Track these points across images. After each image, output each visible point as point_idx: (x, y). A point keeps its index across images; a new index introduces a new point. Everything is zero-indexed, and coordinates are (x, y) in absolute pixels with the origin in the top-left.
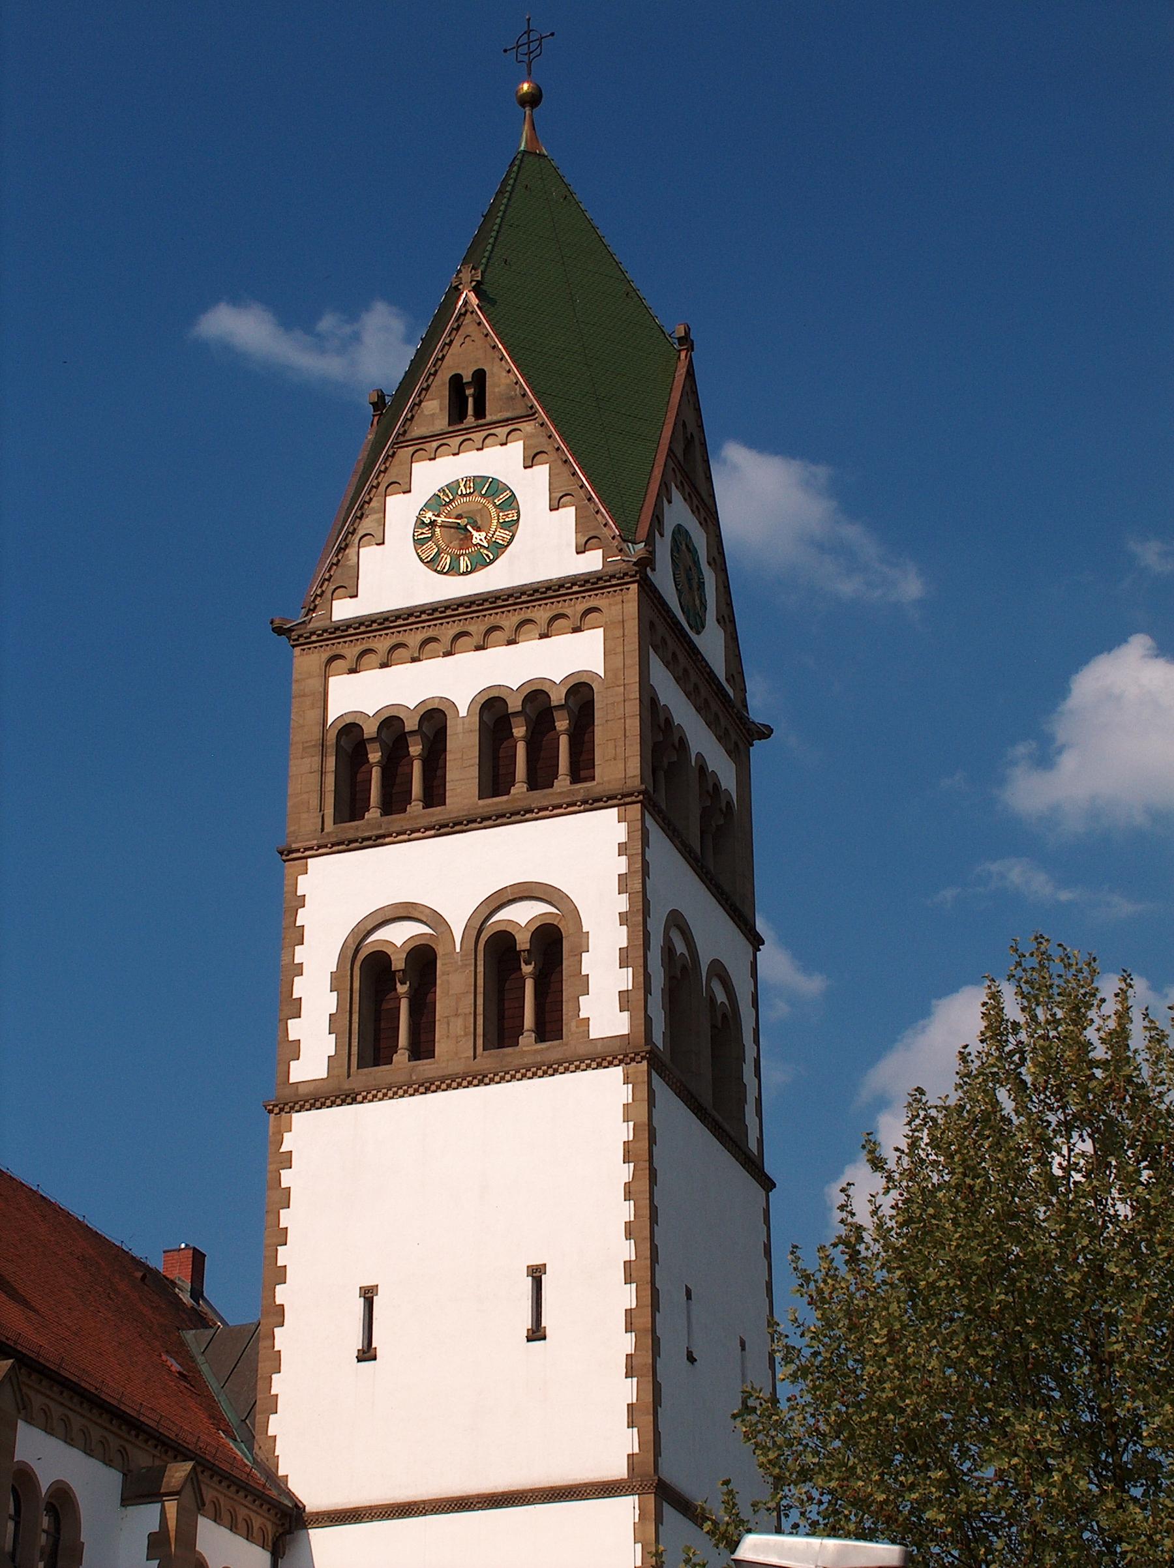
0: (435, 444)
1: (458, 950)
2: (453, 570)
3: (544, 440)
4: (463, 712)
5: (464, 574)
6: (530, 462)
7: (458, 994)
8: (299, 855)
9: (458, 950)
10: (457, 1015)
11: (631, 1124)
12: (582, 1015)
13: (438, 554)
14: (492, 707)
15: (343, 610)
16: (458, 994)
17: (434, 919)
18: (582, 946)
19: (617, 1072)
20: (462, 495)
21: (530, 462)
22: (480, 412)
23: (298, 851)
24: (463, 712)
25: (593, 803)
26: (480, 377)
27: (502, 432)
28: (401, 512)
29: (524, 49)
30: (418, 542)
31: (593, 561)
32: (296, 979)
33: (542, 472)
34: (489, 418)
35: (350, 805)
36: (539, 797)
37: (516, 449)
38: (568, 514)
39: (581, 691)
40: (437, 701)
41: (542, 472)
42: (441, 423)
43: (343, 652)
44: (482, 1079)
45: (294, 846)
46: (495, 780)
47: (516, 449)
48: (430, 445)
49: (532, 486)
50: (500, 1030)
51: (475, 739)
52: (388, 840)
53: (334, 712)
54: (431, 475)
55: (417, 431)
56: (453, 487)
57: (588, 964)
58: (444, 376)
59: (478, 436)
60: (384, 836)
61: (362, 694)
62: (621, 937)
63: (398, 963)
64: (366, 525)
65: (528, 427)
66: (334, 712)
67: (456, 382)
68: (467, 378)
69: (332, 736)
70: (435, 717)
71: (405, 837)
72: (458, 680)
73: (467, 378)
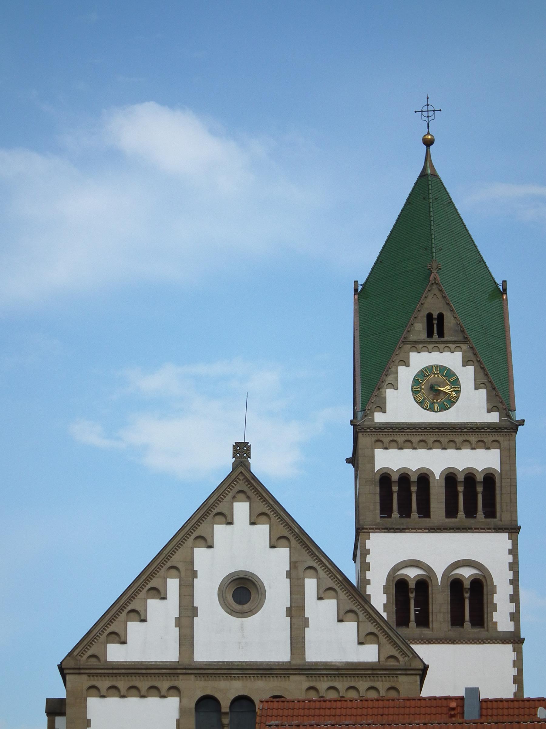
0: (421, 346)
1: (440, 584)
2: (431, 409)
3: (472, 355)
4: (437, 477)
5: (436, 412)
6: (465, 363)
7: (440, 603)
8: (367, 531)
9: (440, 584)
10: (440, 612)
11: (516, 668)
12: (494, 620)
13: (424, 400)
14: (450, 478)
15: (379, 418)
16: (440, 603)
17: (428, 569)
18: (493, 590)
19: (510, 647)
20: (434, 373)
21: (465, 363)
22: (441, 334)
23: (366, 529)
24: (437, 477)
25: (498, 529)
26: (441, 316)
27: (452, 346)
28: (405, 375)
29: (425, 114)
30: (414, 392)
31: (494, 418)
32: (367, 586)
33: (470, 370)
34: (446, 338)
35: (386, 510)
36: (471, 522)
37: (458, 357)
38: (483, 393)
39: (489, 478)
40: (425, 469)
41: (470, 370)
42: (424, 336)
43: (382, 439)
44: (453, 641)
45: (365, 527)
46: (451, 512)
47: (458, 357)
48: (417, 346)
49: (467, 375)
50: (457, 620)
51: (443, 490)
52: (407, 531)
53: (378, 466)
54: (420, 360)
55: (412, 338)
56: (430, 369)
57: (497, 599)
58: (424, 313)
59: (441, 346)
60: (405, 529)
61: (390, 460)
62: (510, 590)
63: (412, 585)
64: (390, 379)
65: (465, 347)
66: (378, 466)
67: (430, 316)
68: (435, 316)
69: (378, 478)
71: (415, 531)
72: (437, 461)
73: (435, 316)
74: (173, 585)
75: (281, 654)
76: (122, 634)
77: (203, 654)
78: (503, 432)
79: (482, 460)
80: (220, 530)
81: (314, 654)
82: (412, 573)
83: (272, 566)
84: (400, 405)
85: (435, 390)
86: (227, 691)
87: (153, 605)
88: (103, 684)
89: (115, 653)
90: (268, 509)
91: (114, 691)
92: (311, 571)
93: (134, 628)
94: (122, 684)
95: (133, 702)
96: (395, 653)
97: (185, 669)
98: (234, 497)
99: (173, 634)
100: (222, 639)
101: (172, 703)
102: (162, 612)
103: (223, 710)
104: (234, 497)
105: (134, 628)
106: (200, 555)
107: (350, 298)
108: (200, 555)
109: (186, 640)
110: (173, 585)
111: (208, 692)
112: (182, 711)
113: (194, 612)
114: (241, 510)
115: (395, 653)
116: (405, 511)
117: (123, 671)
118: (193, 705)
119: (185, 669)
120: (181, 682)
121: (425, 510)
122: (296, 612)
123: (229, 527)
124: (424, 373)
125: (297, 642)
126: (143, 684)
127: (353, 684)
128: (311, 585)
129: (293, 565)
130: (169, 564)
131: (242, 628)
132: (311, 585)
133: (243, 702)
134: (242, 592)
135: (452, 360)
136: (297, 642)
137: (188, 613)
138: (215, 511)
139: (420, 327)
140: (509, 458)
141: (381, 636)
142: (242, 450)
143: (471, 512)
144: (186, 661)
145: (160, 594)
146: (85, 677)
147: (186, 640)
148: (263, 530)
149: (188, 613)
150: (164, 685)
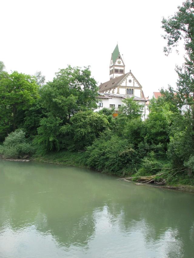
15: (115, 64)
28: (117, 61)
39: (123, 70)
49: (121, 61)
54: (118, 60)
61: (116, 68)
70: (118, 70)
72: (119, 68)
74: (125, 80)
75: (133, 86)
77: (127, 85)
78: (124, 66)
79: (122, 68)
80: (129, 76)
81: (135, 86)
82: (117, 77)
83: (132, 79)
84: (117, 64)
85: (119, 63)
87: (124, 82)
89: (121, 85)
90: (132, 75)
91: (121, 88)
93: (123, 83)
95: (123, 89)
99: (125, 84)
100: (129, 84)
101: (125, 89)
102: (125, 82)
105: (123, 83)
107: (111, 54)
108: (127, 78)
109: (126, 84)
110: (125, 80)
114: (130, 75)
116: (117, 72)
121: (118, 72)
122: (134, 83)
124: (118, 61)
125: (134, 85)
128: (135, 81)
132: (135, 81)
133: (130, 89)
134: (130, 81)
135: (120, 60)
136: (134, 85)
137: (126, 82)
139: (118, 57)
140: (124, 68)
142: (130, 70)
143: (121, 72)
145: (124, 81)
147: (126, 84)
148: (132, 76)
149: (126, 82)
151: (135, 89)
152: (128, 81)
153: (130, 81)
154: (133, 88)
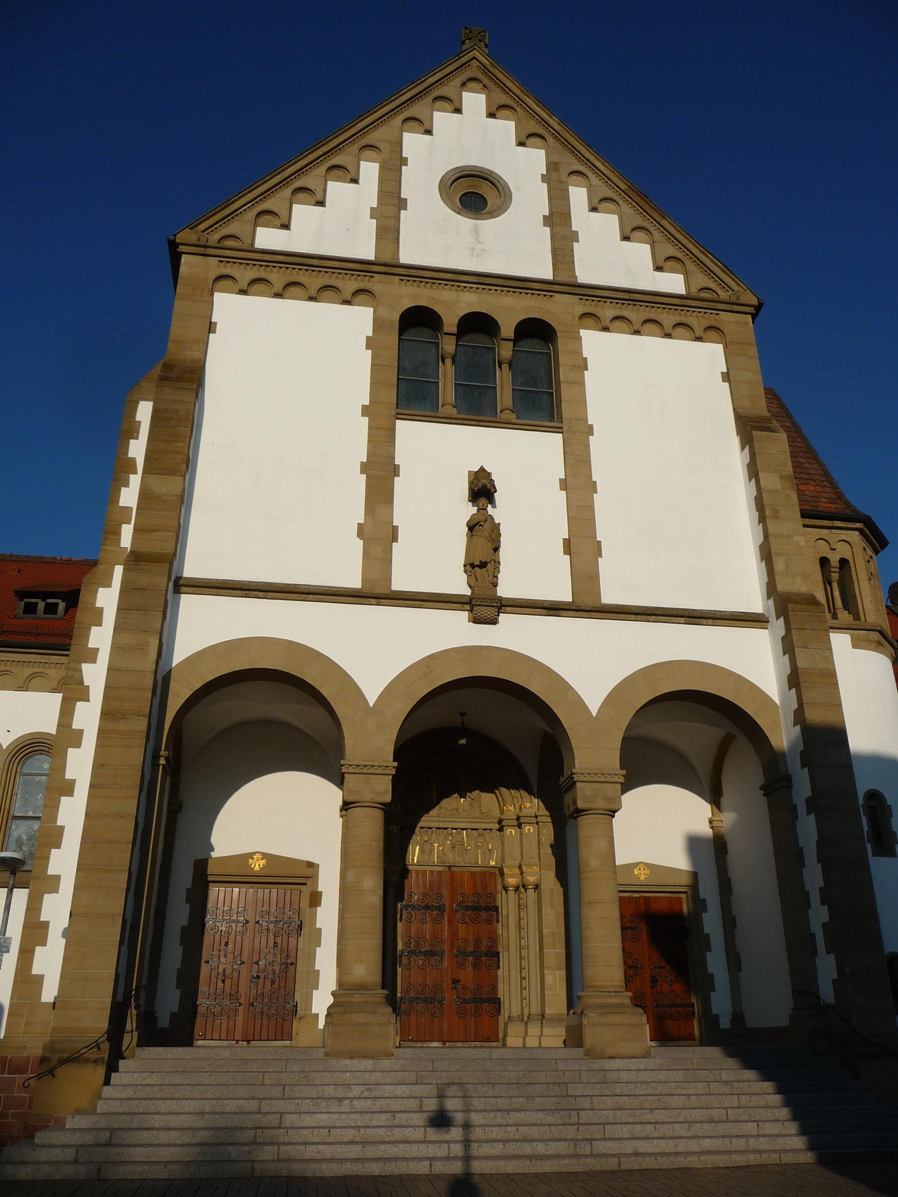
74: (370, 170)
76: (284, 214)
80: (441, 119)
86: (453, 306)
87: (336, 189)
88: (245, 274)
89: (268, 238)
92: (580, 179)
93: (302, 213)
94: (278, 278)
95: (293, 309)
96: (711, 284)
97: (385, 265)
98: (463, 84)
103: (446, 329)
104: (463, 84)
106: (412, 142)
108: (412, 142)
110: (370, 170)
111: (422, 303)
112: (378, 324)
113: (402, 204)
115: (711, 284)
117: (281, 258)
118: (396, 317)
119: (385, 265)
120: (377, 284)
122: (558, 219)
123: (456, 116)
126: (314, 281)
127: (652, 315)
128: (578, 196)
129: (552, 166)
130: (365, 141)
131: (476, 230)
132: (578, 196)
133: (478, 324)
134: (475, 193)
137: (390, 206)
138: (437, 93)
141: (688, 263)
144: (387, 259)
146: (214, 261)
148: (506, 128)
149: (390, 206)
150: (350, 285)
151: (590, 319)
152: (421, 181)
153: (475, 193)
154: (557, 310)
